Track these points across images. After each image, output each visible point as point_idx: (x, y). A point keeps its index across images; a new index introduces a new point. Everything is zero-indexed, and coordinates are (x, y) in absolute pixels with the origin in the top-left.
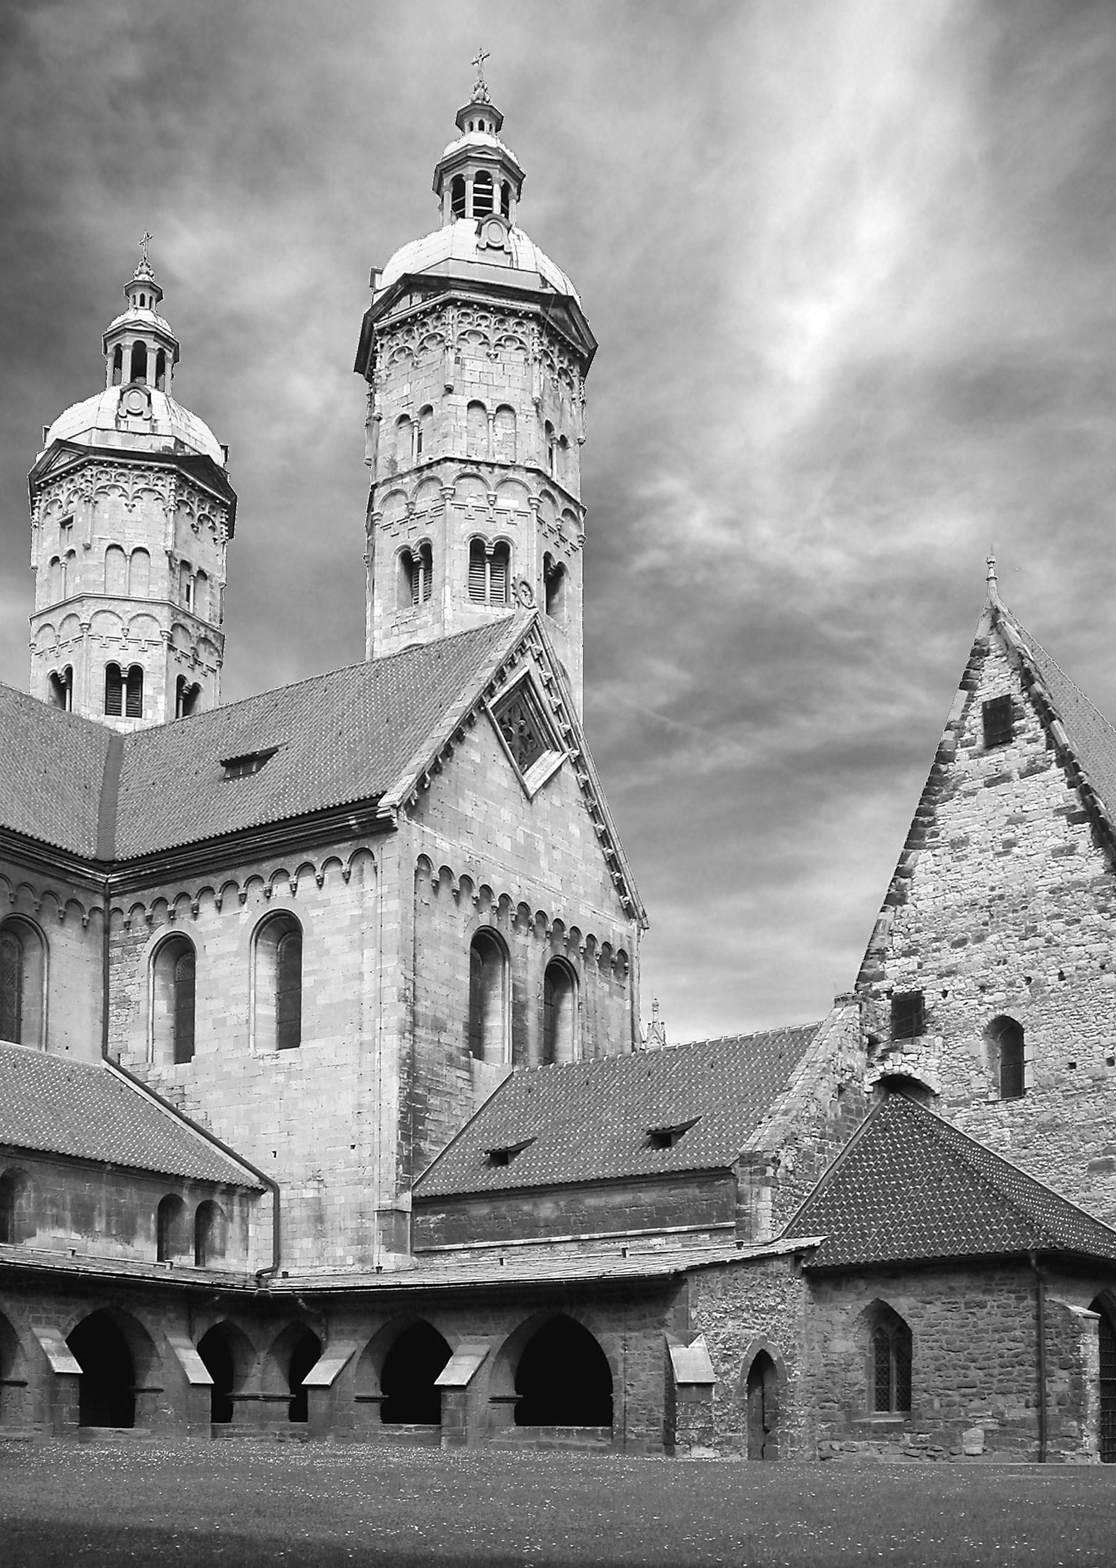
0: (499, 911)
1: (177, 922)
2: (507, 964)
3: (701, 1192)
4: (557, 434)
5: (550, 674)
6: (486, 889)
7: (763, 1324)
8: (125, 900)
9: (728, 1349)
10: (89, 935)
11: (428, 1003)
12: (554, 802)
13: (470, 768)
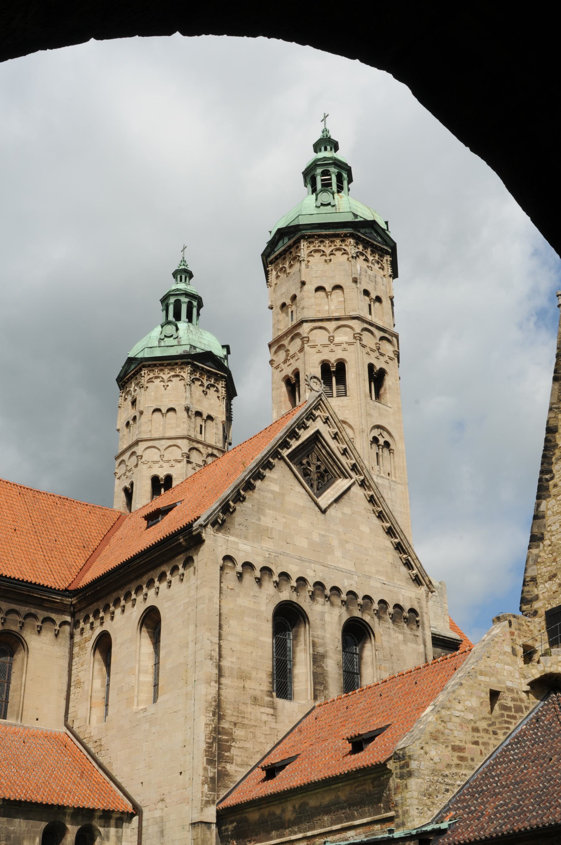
0: (296, 589)
2: (307, 625)
3: (373, 787)
5: (336, 430)
6: (285, 576)
10: (60, 640)
11: (234, 660)
13: (270, 495)
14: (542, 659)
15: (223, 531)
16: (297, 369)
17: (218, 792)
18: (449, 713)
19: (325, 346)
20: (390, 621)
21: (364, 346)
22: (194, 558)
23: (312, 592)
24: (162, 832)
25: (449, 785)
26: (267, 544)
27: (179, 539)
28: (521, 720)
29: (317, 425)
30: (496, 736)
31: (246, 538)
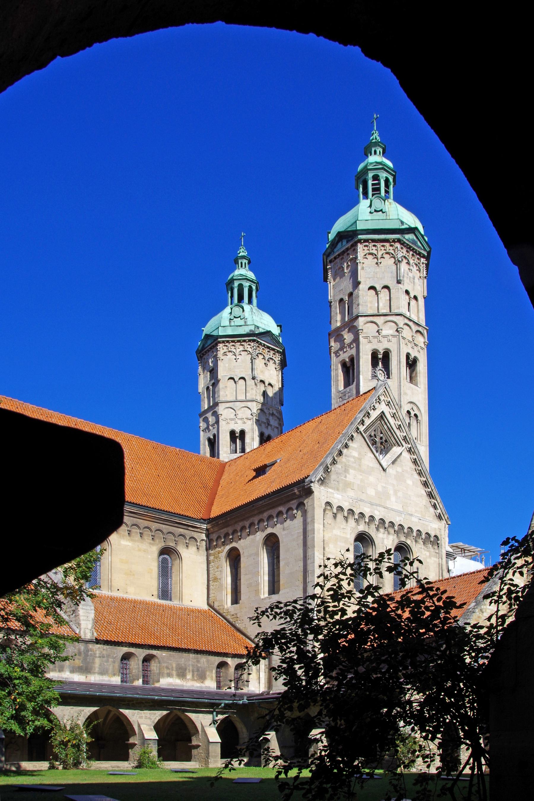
4: (412, 295)
6: (362, 515)
8: (214, 535)
12: (398, 470)
13: (352, 460)
15: (324, 485)
19: (374, 337)
21: (404, 338)
22: (305, 502)
23: (378, 526)
26: (350, 493)
27: (294, 490)
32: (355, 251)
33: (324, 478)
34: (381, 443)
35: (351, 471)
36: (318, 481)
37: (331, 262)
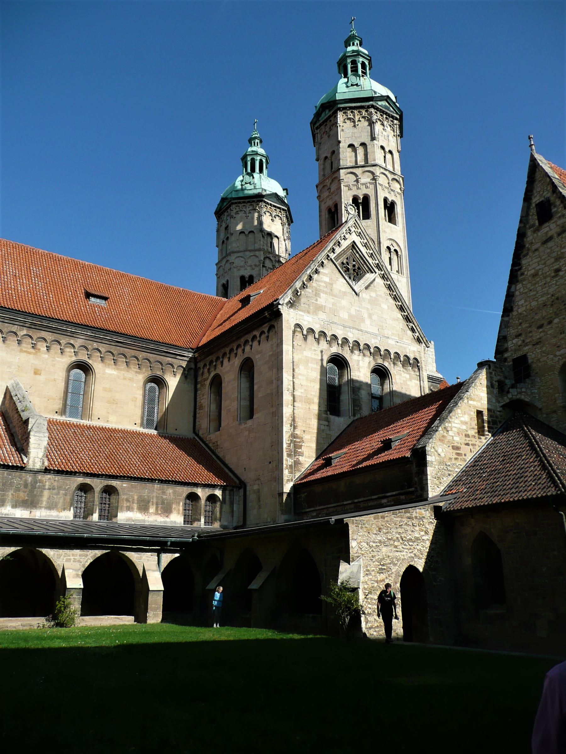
1: (217, 369)
5: (366, 241)
6: (335, 337)
7: (410, 549)
8: (201, 363)
9: (383, 565)
11: (303, 391)
13: (323, 284)
14: (511, 390)
16: (336, 201)
17: (295, 474)
18: (450, 425)
20: (401, 365)
21: (380, 185)
23: (352, 347)
24: (259, 499)
25: (451, 471)
26: (322, 316)
27: (265, 314)
28: (496, 430)
29: (354, 237)
30: (480, 440)
31: (308, 312)
32: (336, 117)
33: (294, 302)
34: (354, 270)
35: (322, 295)
36: (287, 304)
37: (317, 128)
